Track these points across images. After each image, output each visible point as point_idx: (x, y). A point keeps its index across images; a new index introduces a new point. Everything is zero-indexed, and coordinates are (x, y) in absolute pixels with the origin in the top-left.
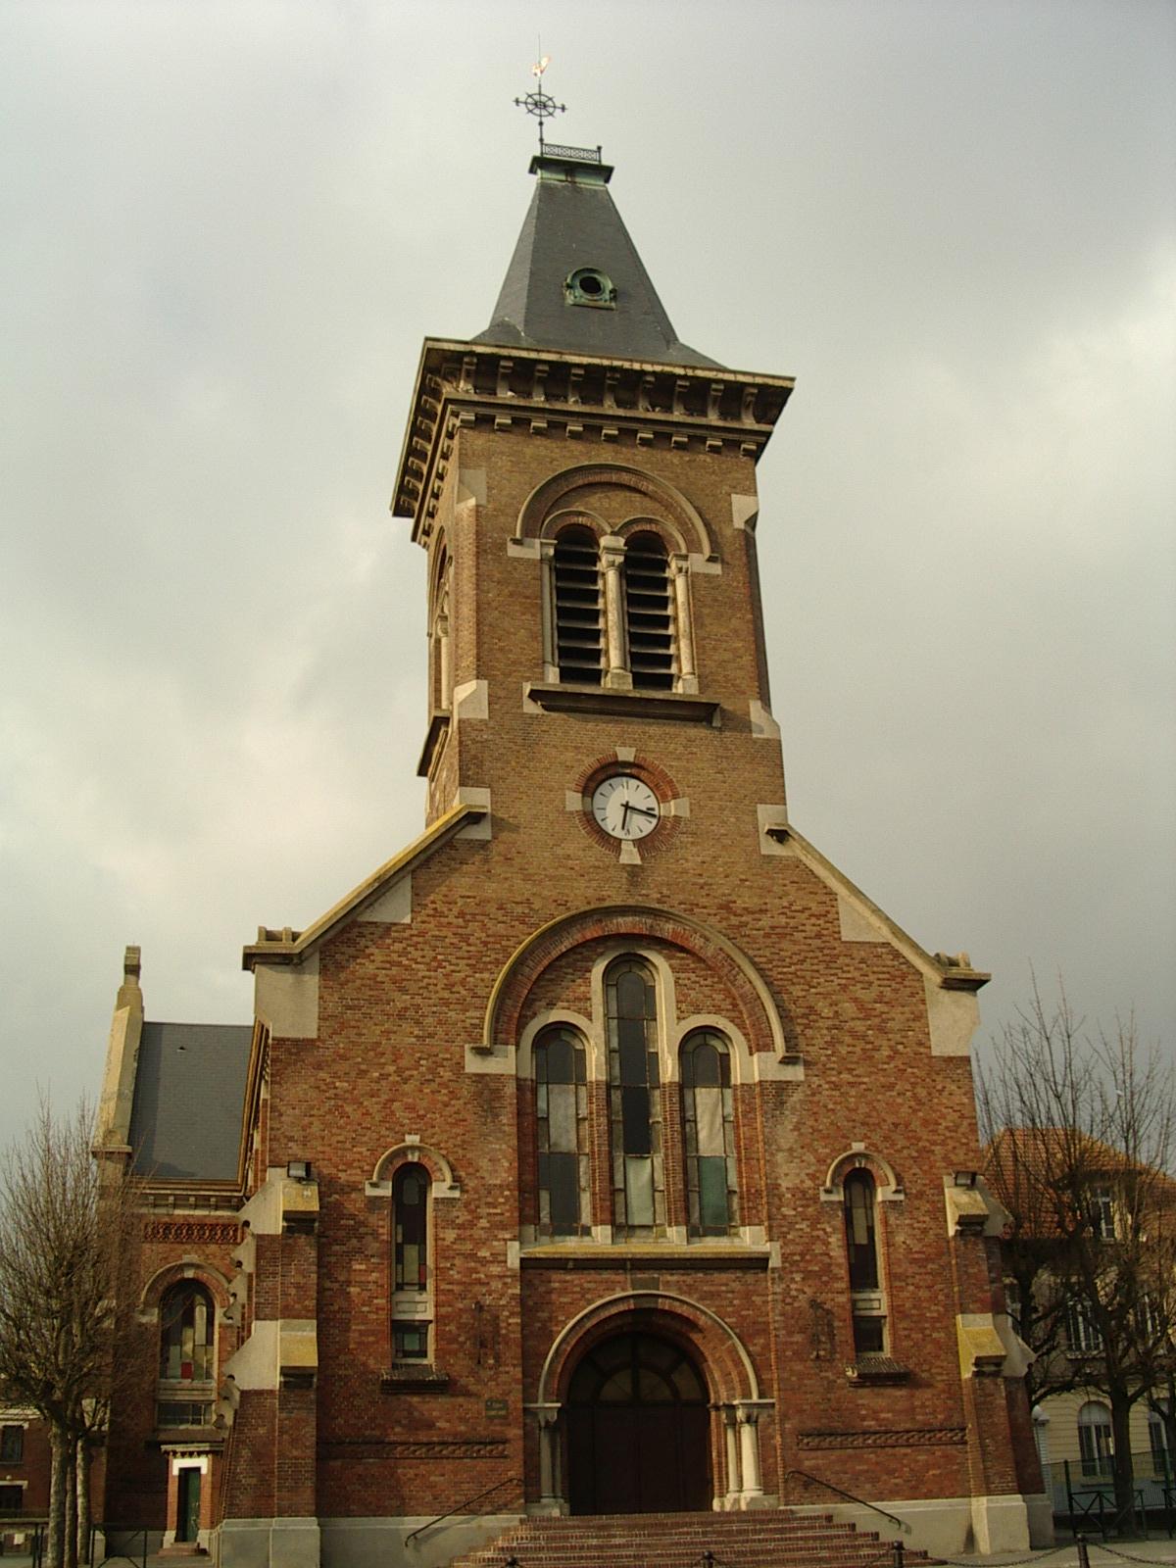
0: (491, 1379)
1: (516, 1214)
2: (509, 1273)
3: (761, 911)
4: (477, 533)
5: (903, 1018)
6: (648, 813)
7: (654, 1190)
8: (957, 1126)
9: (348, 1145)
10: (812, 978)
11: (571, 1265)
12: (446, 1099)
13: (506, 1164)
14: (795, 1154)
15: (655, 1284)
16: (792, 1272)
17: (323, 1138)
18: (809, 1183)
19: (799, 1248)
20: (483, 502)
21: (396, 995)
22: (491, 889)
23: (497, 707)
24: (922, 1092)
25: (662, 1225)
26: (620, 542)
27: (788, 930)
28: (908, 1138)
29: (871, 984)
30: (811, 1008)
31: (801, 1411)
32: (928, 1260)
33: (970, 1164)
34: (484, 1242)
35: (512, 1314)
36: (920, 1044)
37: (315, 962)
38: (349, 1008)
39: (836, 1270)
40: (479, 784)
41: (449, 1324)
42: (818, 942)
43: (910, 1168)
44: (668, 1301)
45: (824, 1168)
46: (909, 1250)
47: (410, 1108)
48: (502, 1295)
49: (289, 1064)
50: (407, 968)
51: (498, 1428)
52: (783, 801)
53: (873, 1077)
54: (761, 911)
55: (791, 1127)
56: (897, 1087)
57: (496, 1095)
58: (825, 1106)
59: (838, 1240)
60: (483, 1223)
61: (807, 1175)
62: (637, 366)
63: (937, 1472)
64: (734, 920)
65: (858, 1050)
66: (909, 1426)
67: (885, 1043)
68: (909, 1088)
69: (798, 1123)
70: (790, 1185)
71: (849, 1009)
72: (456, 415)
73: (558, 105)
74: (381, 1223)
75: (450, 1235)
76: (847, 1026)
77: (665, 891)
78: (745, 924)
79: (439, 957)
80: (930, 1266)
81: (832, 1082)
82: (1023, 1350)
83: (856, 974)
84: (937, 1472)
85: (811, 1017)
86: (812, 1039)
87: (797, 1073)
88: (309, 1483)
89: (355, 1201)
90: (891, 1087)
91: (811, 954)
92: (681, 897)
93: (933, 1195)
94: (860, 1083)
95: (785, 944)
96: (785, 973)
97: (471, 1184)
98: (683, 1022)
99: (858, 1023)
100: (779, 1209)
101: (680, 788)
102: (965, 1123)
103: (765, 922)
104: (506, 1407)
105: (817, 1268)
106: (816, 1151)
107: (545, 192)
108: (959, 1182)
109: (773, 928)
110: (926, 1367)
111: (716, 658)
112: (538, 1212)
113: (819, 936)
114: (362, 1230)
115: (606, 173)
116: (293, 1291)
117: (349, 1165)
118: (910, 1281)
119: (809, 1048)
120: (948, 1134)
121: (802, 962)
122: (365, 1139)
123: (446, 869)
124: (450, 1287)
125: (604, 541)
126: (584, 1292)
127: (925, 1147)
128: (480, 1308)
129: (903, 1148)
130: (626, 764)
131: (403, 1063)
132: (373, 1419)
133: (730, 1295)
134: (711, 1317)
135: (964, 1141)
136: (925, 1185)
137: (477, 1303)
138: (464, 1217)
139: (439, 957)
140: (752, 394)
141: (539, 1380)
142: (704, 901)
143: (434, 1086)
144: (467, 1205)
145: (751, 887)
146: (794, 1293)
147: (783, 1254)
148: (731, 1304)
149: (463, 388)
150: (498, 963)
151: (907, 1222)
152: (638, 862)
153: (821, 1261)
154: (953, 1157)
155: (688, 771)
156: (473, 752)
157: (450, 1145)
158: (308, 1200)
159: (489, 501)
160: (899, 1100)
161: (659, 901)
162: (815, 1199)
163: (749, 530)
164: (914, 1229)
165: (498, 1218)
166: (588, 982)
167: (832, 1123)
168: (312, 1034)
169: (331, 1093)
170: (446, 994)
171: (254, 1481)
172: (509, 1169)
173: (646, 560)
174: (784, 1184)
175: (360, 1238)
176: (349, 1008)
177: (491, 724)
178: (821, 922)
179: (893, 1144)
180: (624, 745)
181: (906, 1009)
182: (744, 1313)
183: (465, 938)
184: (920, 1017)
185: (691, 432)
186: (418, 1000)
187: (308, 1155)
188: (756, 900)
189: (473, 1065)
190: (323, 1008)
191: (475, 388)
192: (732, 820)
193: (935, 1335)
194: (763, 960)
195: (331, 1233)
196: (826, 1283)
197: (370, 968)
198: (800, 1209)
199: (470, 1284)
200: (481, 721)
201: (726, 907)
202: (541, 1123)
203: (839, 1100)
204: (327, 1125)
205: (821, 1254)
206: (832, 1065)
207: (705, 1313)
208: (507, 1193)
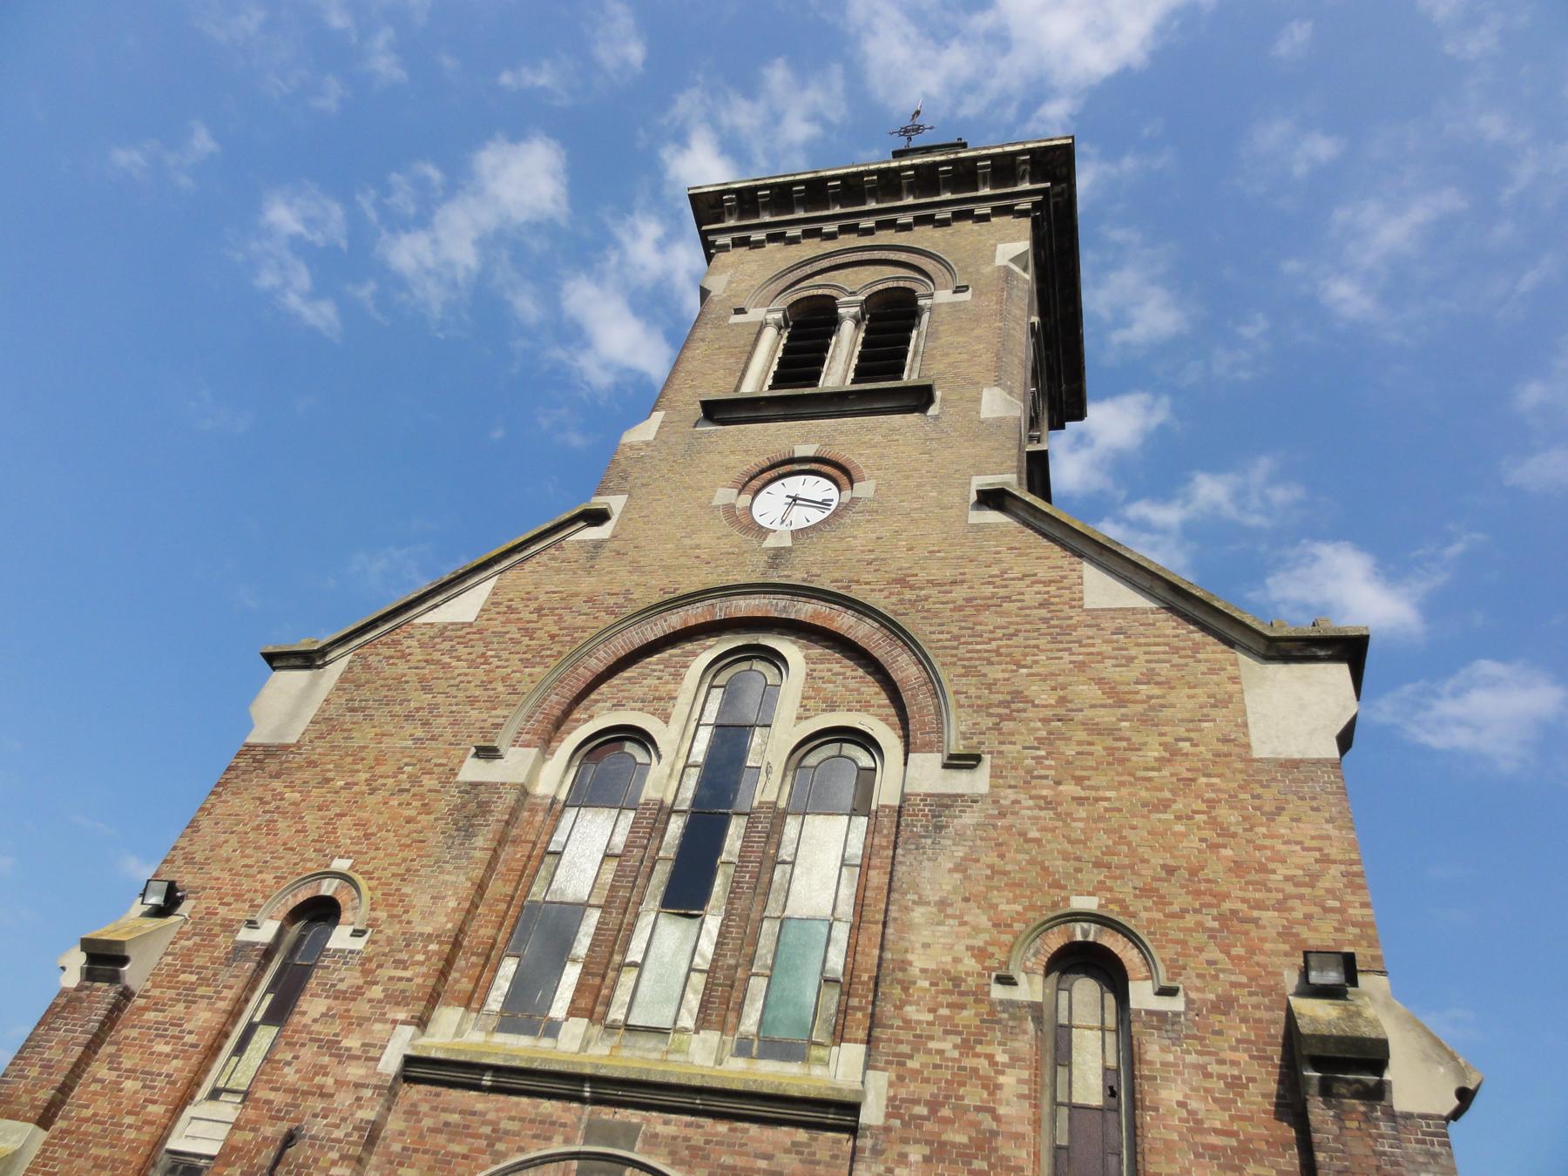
2: (374, 1081)
3: (954, 583)
5: (1191, 704)
7: (691, 969)
8: (1313, 879)
10: (1026, 655)
13: (452, 904)
14: (949, 911)
16: (905, 1141)
18: (970, 964)
19: (928, 1091)
22: (587, 584)
24: (1229, 817)
25: (686, 1030)
27: (995, 601)
28: (1197, 893)
29: (1131, 659)
30: (1017, 695)
34: (362, 1021)
39: (1006, 1148)
41: (233, 1164)
42: (1043, 612)
43: (1200, 950)
45: (1007, 938)
46: (1197, 1126)
48: (344, 1119)
49: (245, 772)
50: (445, 666)
53: (1124, 791)
54: (954, 583)
55: (951, 865)
56: (1175, 806)
57: (484, 808)
59: (1020, 1081)
60: (376, 992)
61: (969, 948)
64: (909, 595)
65: (1098, 749)
68: (1204, 807)
69: (964, 859)
70: (932, 966)
71: (1086, 692)
76: (1079, 716)
77: (815, 570)
81: (1044, 798)
86: (1012, 734)
87: (976, 782)
92: (837, 575)
93: (1256, 1007)
94: (1097, 800)
96: (979, 651)
97: (390, 932)
99: (1103, 711)
100: (899, 1007)
101: (866, 472)
102: (1335, 870)
103: (959, 593)
106: (994, 907)
108: (1315, 977)
116: (33, 1072)
117: (239, 897)
120: (1290, 889)
121: (1010, 636)
122: (281, 863)
124: (272, 1095)
126: (498, 1134)
127: (1234, 912)
129: (1184, 911)
136: (1234, 985)
140: (1024, 162)
143: (406, 797)
147: (891, 1100)
151: (1192, 1058)
153: (975, 1125)
154: (1304, 933)
160: (1179, 828)
162: (980, 995)
164: (1208, 1075)
165: (402, 985)
166: (678, 677)
167: (1032, 862)
172: (454, 910)
176: (352, 710)
178: (1052, 589)
181: (1198, 691)
186: (440, 699)
189: (473, 770)
198: (944, 1012)
199: (305, 1093)
201: (902, 581)
203: (1050, 824)
204: (243, 844)
205: (978, 1109)
206: (1043, 772)
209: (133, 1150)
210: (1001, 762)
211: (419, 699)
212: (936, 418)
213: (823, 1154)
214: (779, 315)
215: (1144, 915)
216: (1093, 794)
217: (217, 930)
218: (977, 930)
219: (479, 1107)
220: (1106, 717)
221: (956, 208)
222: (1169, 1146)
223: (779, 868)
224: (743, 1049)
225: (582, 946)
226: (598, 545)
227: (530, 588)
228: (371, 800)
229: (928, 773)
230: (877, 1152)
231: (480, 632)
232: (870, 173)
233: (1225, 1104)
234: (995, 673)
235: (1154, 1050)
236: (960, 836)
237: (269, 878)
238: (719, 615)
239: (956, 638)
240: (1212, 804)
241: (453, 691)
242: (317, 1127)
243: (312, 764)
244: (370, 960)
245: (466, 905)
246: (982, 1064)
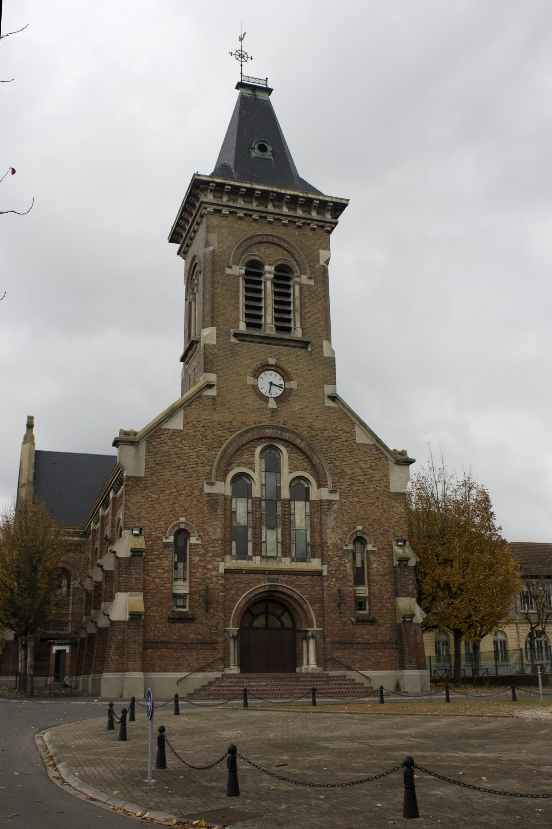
0: (212, 618)
1: (223, 551)
4: (213, 262)
6: (279, 386)
7: (277, 543)
8: (399, 521)
9: (156, 521)
11: (244, 572)
12: (196, 503)
13: (219, 530)
15: (277, 580)
16: (331, 578)
17: (146, 518)
18: (339, 542)
19: (334, 568)
20: (216, 248)
21: (177, 459)
22: (216, 417)
23: (220, 339)
24: (385, 507)
26: (272, 269)
29: (367, 461)
31: (334, 634)
32: (385, 575)
33: (403, 537)
34: (210, 562)
35: (221, 591)
36: (386, 487)
37: (143, 446)
38: (157, 464)
39: (349, 577)
40: (212, 372)
42: (347, 443)
44: (282, 588)
46: (378, 571)
47: (181, 506)
50: (181, 448)
51: (214, 637)
52: (335, 384)
53: (366, 500)
56: (376, 504)
58: (347, 511)
60: (210, 554)
62: (283, 191)
63: (385, 660)
64: (313, 433)
65: (361, 488)
66: (375, 641)
67: (371, 486)
70: (332, 543)
71: (358, 471)
72: (206, 208)
73: (249, 56)
74: (169, 553)
75: (196, 559)
76: (357, 478)
77: (286, 420)
78: (317, 435)
79: (195, 444)
80: (386, 577)
82: (421, 613)
83: (361, 457)
84: (385, 660)
85: (343, 474)
87: (336, 497)
88: (140, 659)
89: (159, 544)
90: (373, 504)
91: (344, 448)
92: (292, 422)
95: (333, 444)
98: (291, 474)
99: (361, 477)
101: (293, 377)
102: (403, 519)
103: (326, 434)
104: (217, 629)
105: (341, 576)
107: (242, 100)
109: (329, 437)
110: (382, 618)
111: (310, 321)
112: (231, 549)
113: (347, 441)
114: (161, 556)
115: (269, 91)
116: (134, 581)
117: (157, 529)
118: (378, 583)
119: (341, 487)
120: (395, 524)
121: (340, 451)
122: (163, 519)
123: (197, 407)
124: (196, 580)
125: (267, 268)
126: (249, 583)
128: (207, 588)
130: (271, 365)
131: (178, 488)
132: (164, 633)
133: (306, 586)
134: (299, 595)
135: (402, 527)
137: (207, 587)
138: (202, 551)
139: (195, 444)
140: (331, 206)
141: (230, 618)
142: (301, 424)
144: (203, 547)
145: (320, 419)
146: (332, 586)
148: (307, 590)
149: (210, 197)
150: (218, 447)
152: (276, 407)
154: (397, 533)
155: (297, 370)
156: (210, 358)
157: (197, 522)
158: (140, 543)
159: (218, 248)
160: (376, 510)
161: (284, 424)
162: (342, 548)
163: (326, 265)
165: (216, 552)
166: (253, 456)
168: (143, 475)
169: (150, 499)
170: (197, 460)
171: (117, 657)
173: (283, 275)
174: (330, 542)
175: (161, 559)
176: (157, 464)
177: (217, 346)
178: (348, 435)
179: (373, 527)
180: (271, 357)
181: (381, 472)
182: (312, 593)
183: (205, 437)
184: (386, 476)
185: (304, 221)
186: (186, 462)
187: (140, 525)
188: (322, 425)
189: (207, 489)
190: (147, 464)
191: (214, 196)
192: (314, 391)
193: (387, 605)
194: (324, 450)
195: (149, 557)
196: (345, 583)
197: (166, 448)
198: (335, 552)
200: (213, 345)
201: (310, 427)
202: (233, 513)
203: (352, 508)
207: (296, 593)
208: (219, 542)
209: (168, 595)
210: (341, 491)
211: (179, 462)
212: (311, 352)
213: (315, 580)
214: (243, 272)
215: (370, 530)
216: (360, 501)
217: (156, 539)
218: (340, 534)
219: (243, 577)
220: (362, 479)
221: (304, 221)
222: (374, 574)
223: (292, 516)
224: (293, 560)
225: (250, 538)
226: (214, 398)
227: (197, 416)
228: (182, 498)
229: (325, 494)
230: (327, 580)
231: (187, 434)
232: (273, 192)
233: (382, 567)
234: (338, 463)
235: (372, 558)
236: (334, 511)
237: (163, 523)
238: (262, 435)
239: (327, 450)
240: (383, 503)
241: (189, 459)
242: (211, 586)
243: (154, 484)
244: (204, 546)
245: (223, 531)
246: (343, 562)
